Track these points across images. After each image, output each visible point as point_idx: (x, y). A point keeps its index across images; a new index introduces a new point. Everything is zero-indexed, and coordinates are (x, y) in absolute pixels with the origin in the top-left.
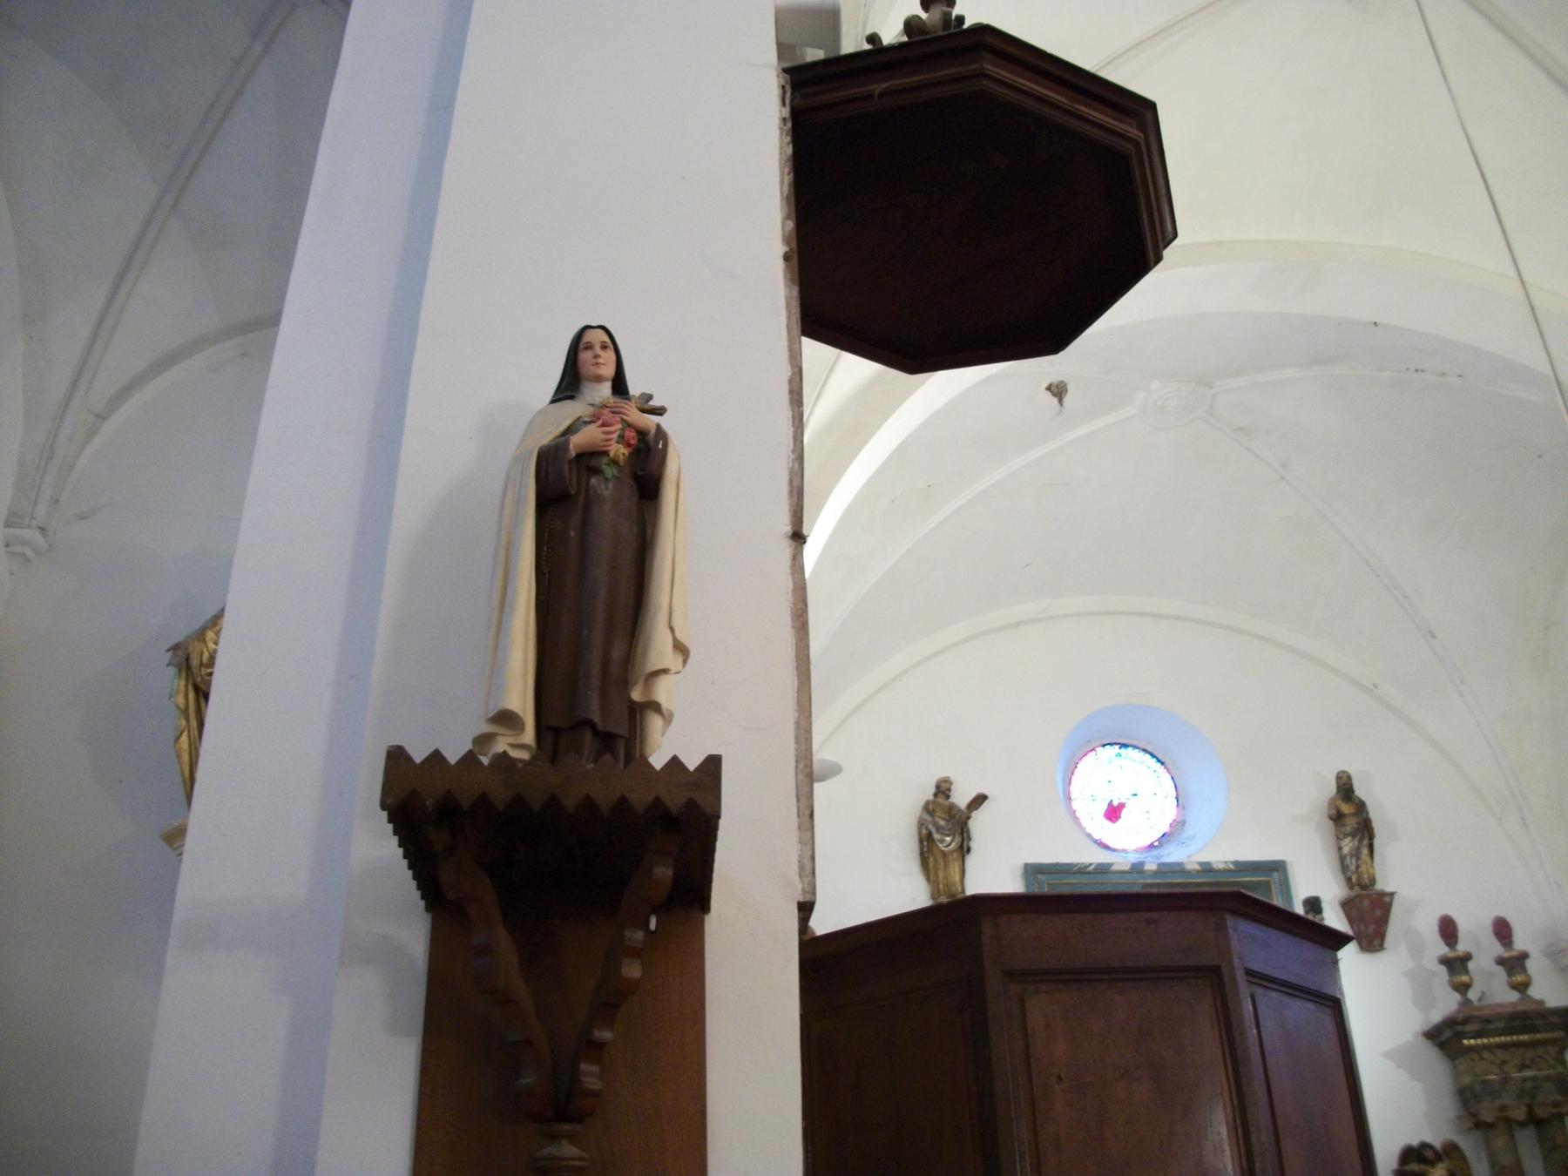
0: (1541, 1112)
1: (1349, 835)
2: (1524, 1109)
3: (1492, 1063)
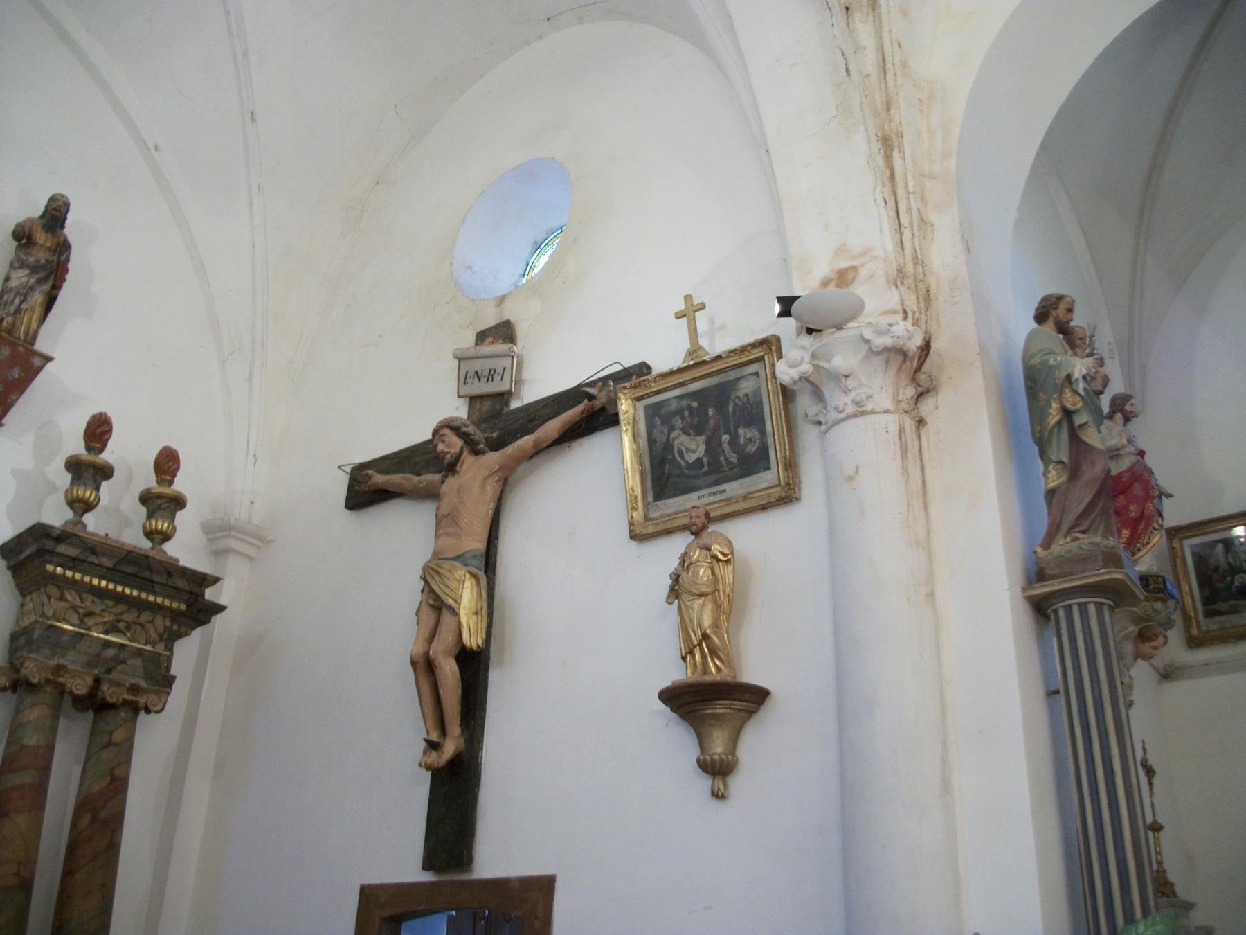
0: (109, 692)
1: (28, 267)
2: (90, 681)
3: (74, 608)
